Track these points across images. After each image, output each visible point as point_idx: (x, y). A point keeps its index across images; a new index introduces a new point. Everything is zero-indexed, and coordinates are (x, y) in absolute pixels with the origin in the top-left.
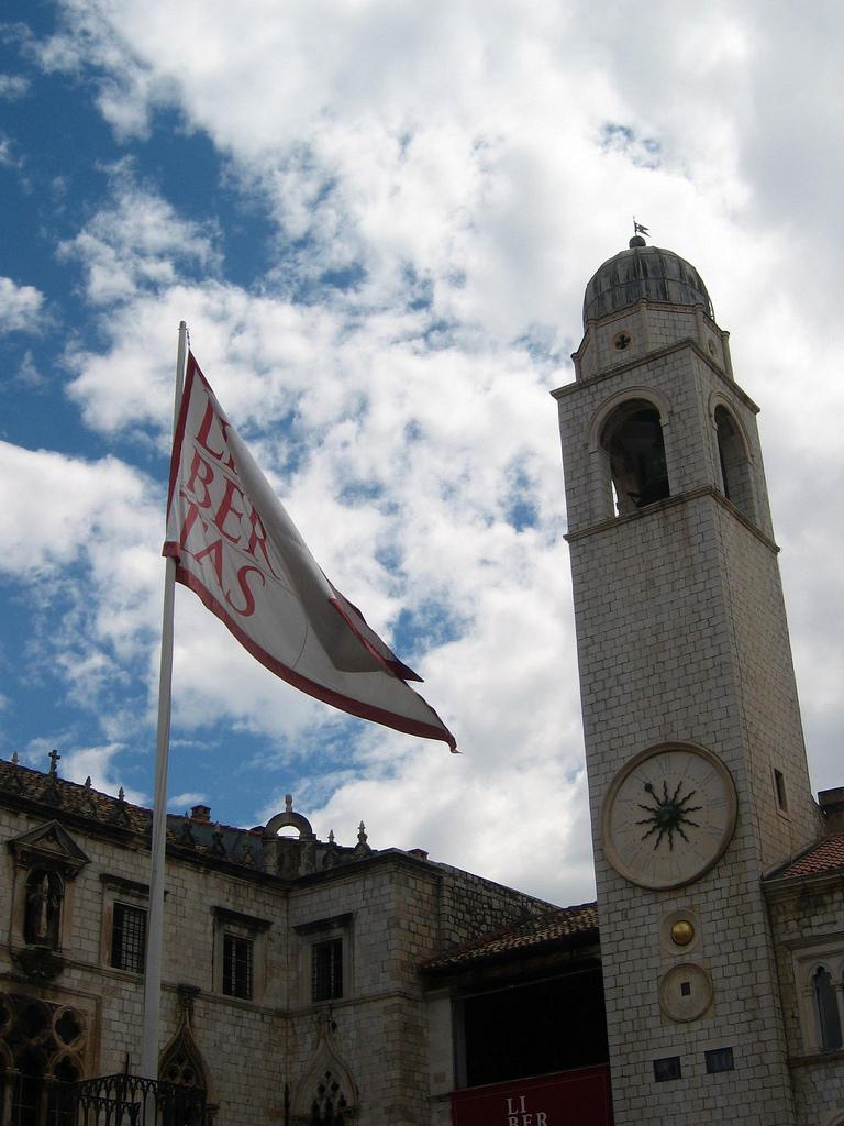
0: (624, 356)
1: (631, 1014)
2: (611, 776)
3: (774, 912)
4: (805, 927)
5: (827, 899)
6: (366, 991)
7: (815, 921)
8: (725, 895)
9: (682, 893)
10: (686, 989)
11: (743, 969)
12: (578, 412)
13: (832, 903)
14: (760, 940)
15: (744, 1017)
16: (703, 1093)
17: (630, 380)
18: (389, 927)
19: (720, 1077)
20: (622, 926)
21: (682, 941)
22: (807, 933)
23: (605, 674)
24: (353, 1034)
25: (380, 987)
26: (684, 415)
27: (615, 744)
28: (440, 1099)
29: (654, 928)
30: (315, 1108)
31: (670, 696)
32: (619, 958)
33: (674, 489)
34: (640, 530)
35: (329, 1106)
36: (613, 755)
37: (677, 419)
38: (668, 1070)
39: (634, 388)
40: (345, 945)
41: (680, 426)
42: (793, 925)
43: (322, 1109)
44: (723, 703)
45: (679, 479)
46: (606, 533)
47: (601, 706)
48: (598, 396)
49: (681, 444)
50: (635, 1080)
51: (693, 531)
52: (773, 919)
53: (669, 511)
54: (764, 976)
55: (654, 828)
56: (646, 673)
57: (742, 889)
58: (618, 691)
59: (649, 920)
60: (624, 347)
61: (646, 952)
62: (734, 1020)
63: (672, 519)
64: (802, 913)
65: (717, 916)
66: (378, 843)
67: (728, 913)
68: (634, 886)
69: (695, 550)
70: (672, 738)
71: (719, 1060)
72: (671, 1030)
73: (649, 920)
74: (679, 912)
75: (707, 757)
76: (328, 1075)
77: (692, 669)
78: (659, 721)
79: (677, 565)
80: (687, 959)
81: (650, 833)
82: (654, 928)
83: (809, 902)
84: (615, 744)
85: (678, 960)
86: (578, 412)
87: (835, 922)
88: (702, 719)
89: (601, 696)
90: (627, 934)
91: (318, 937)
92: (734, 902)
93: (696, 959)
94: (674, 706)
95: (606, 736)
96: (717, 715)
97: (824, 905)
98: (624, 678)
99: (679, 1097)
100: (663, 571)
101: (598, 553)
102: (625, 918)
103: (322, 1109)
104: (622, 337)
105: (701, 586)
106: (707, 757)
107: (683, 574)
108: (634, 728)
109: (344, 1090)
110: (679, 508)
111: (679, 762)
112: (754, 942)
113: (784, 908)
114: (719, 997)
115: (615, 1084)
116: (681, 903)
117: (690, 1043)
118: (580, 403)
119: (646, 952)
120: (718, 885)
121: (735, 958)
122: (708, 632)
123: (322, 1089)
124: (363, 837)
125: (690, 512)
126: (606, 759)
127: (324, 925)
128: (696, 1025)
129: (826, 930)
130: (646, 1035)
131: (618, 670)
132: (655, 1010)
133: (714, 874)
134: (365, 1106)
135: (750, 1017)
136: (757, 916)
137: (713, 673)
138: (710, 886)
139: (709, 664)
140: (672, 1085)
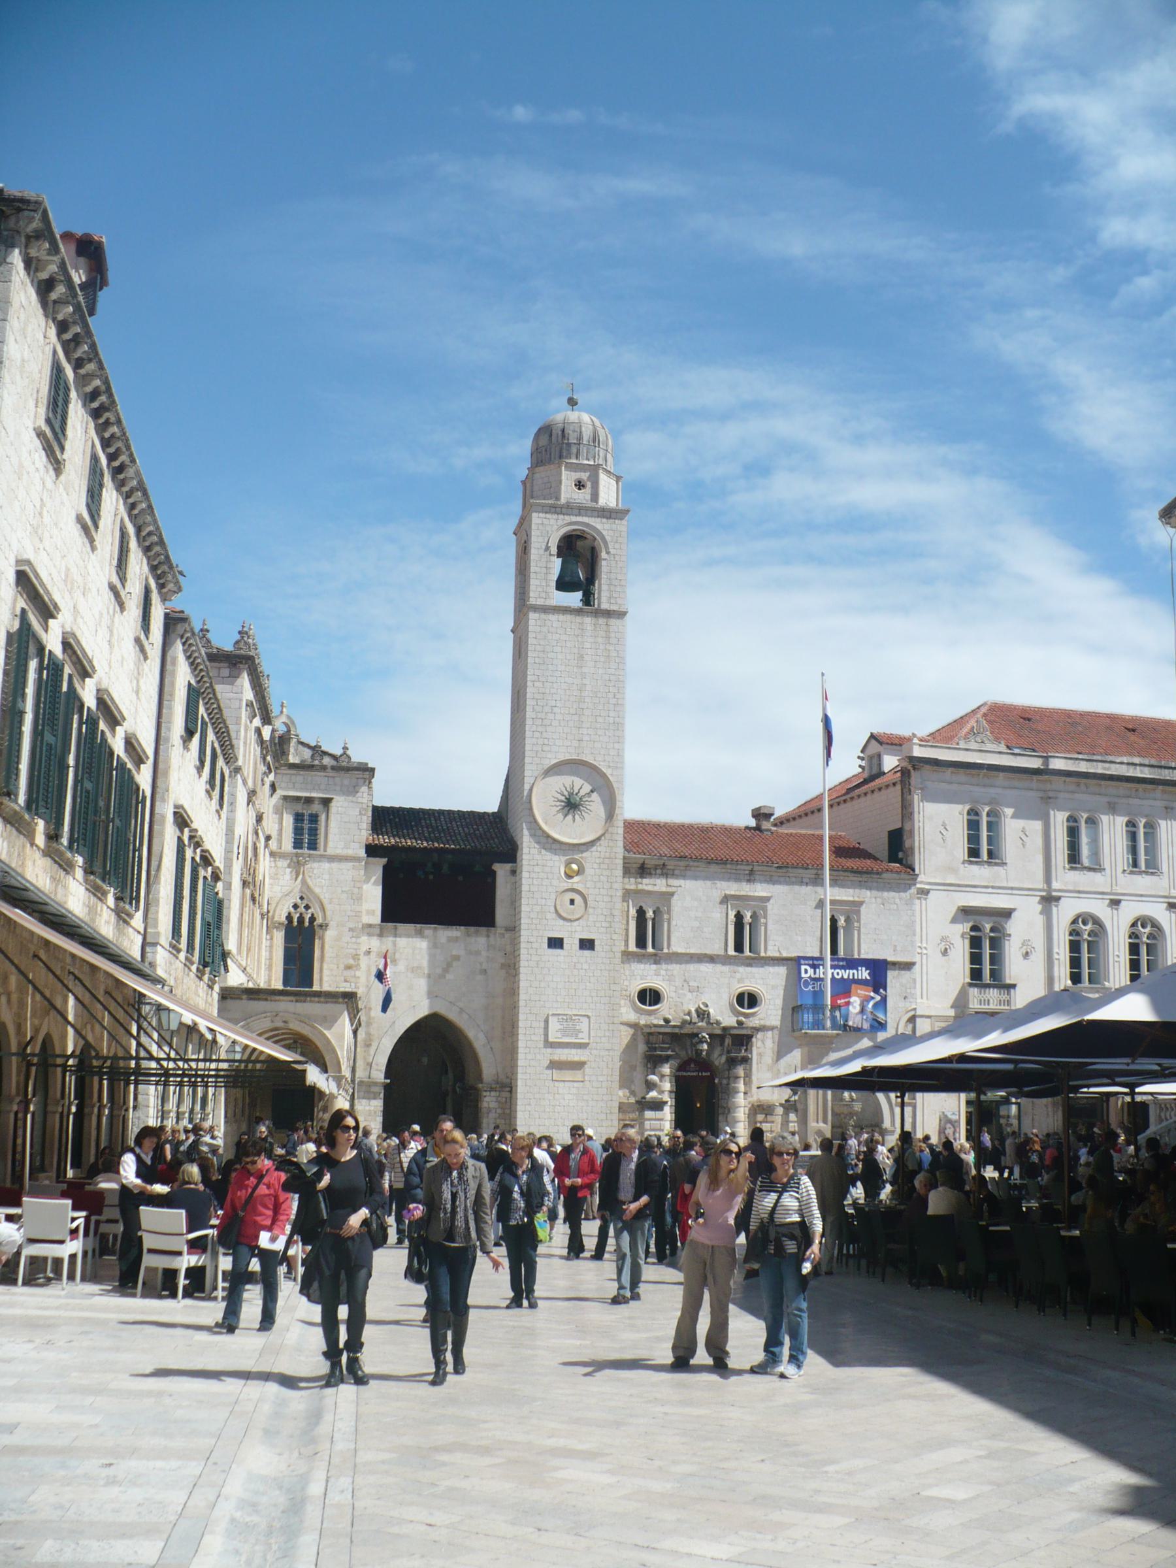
1: (538, 908)
6: (339, 852)
7: (645, 881)
8: (602, 855)
10: (572, 902)
11: (607, 899)
15: (604, 924)
16: (575, 960)
18: (361, 814)
19: (587, 953)
24: (326, 877)
25: (350, 852)
26: (617, 558)
27: (545, 748)
28: (370, 926)
30: (289, 917)
32: (533, 875)
35: (301, 919)
38: (556, 943)
39: (587, 525)
40: (323, 817)
41: (613, 563)
43: (295, 920)
44: (616, 745)
47: (539, 722)
48: (561, 517)
49: (613, 576)
50: (534, 945)
51: (613, 635)
57: (613, 855)
58: (551, 716)
62: (598, 924)
65: (596, 866)
66: (356, 757)
67: (603, 866)
69: (612, 648)
71: (587, 944)
72: (561, 922)
75: (604, 775)
76: (302, 898)
77: (600, 720)
80: (575, 886)
84: (545, 748)
88: (603, 752)
91: (299, 808)
92: (607, 861)
94: (586, 738)
95: (540, 741)
97: (650, 874)
99: (561, 959)
100: (589, 652)
103: (295, 920)
107: (602, 659)
109: (315, 910)
114: (591, 911)
115: (523, 945)
117: (571, 935)
119: (550, 876)
121: (603, 892)
122: (613, 701)
123: (295, 906)
124: (345, 748)
127: (309, 800)
128: (576, 923)
130: (545, 922)
131: (553, 703)
132: (553, 909)
134: (332, 924)
135: (607, 925)
138: (594, 848)
139: (611, 720)
140: (558, 951)
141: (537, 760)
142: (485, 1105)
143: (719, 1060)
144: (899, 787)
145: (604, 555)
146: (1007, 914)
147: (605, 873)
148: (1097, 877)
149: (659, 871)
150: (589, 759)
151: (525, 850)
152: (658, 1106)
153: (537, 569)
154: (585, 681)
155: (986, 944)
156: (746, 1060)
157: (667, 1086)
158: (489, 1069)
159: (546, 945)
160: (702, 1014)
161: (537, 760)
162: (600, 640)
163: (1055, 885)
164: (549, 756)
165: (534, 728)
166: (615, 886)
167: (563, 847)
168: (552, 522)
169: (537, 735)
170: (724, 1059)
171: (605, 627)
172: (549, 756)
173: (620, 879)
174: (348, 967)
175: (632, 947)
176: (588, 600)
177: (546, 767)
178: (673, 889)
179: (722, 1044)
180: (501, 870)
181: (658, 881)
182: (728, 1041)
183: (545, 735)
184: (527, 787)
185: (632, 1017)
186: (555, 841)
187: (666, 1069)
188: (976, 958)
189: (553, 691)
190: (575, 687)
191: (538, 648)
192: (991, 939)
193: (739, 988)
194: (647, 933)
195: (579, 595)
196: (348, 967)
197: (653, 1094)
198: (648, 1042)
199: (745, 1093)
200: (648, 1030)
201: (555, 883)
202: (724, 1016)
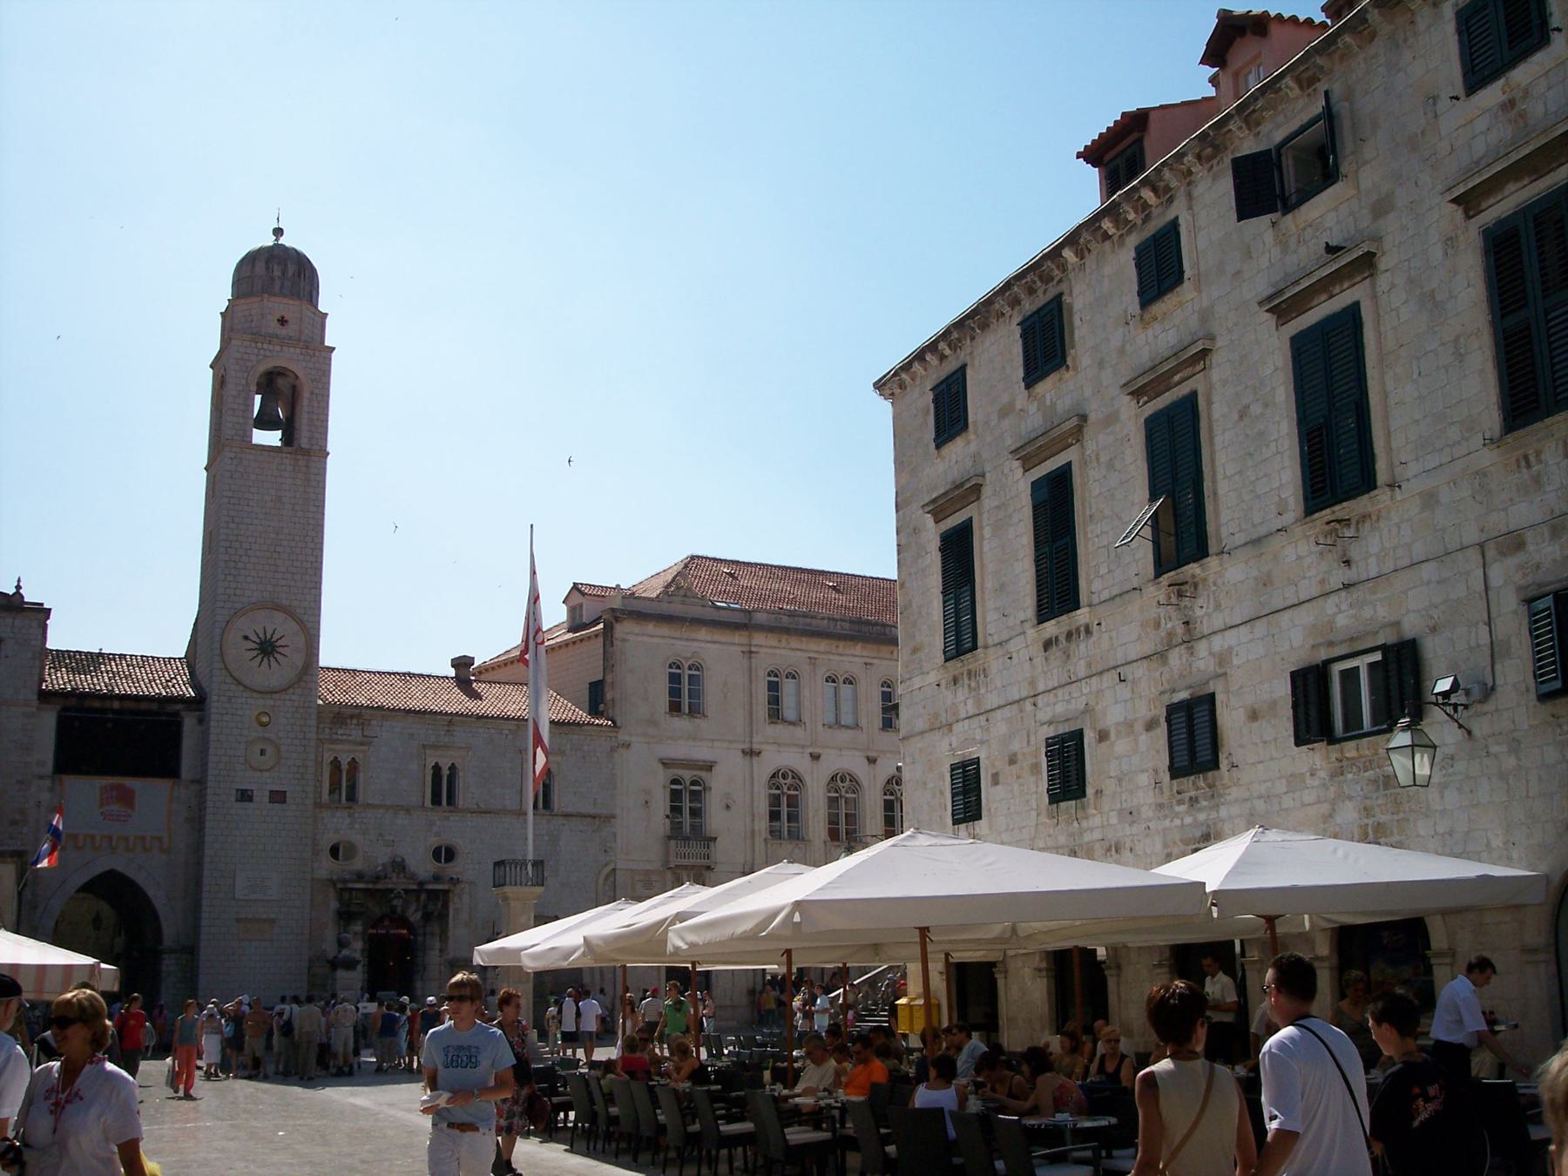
0: (283, 331)
10: (263, 752)
14: (312, 736)
21: (264, 725)
23: (237, 545)
28: (41, 777)
38: (245, 796)
45: (310, 439)
54: (312, 757)
66: (30, 596)
69: (310, 490)
71: (278, 797)
75: (300, 622)
78: (269, 588)
95: (233, 585)
102: (230, 698)
106: (300, 622)
111: (279, 617)
117: (262, 785)
121: (296, 742)
124: (18, 587)
136: (314, 722)
142: (164, 968)
143: (415, 916)
144: (601, 639)
146: (709, 767)
148: (799, 732)
150: (285, 602)
151: (215, 698)
152: (350, 964)
155: (686, 797)
156: (443, 917)
157: (358, 945)
158: (171, 929)
159: (233, 799)
160: (399, 866)
162: (299, 482)
163: (756, 739)
168: (253, 358)
170: (419, 915)
173: (314, 729)
174: (14, 823)
175: (325, 796)
176: (288, 439)
179: (418, 899)
180: (189, 722)
182: (423, 897)
185: (322, 873)
187: (358, 927)
188: (676, 810)
192: (693, 793)
193: (434, 841)
194: (344, 784)
195: (279, 433)
196: (14, 823)
197: (345, 952)
198: (340, 899)
199: (441, 950)
200: (340, 886)
202: (422, 866)
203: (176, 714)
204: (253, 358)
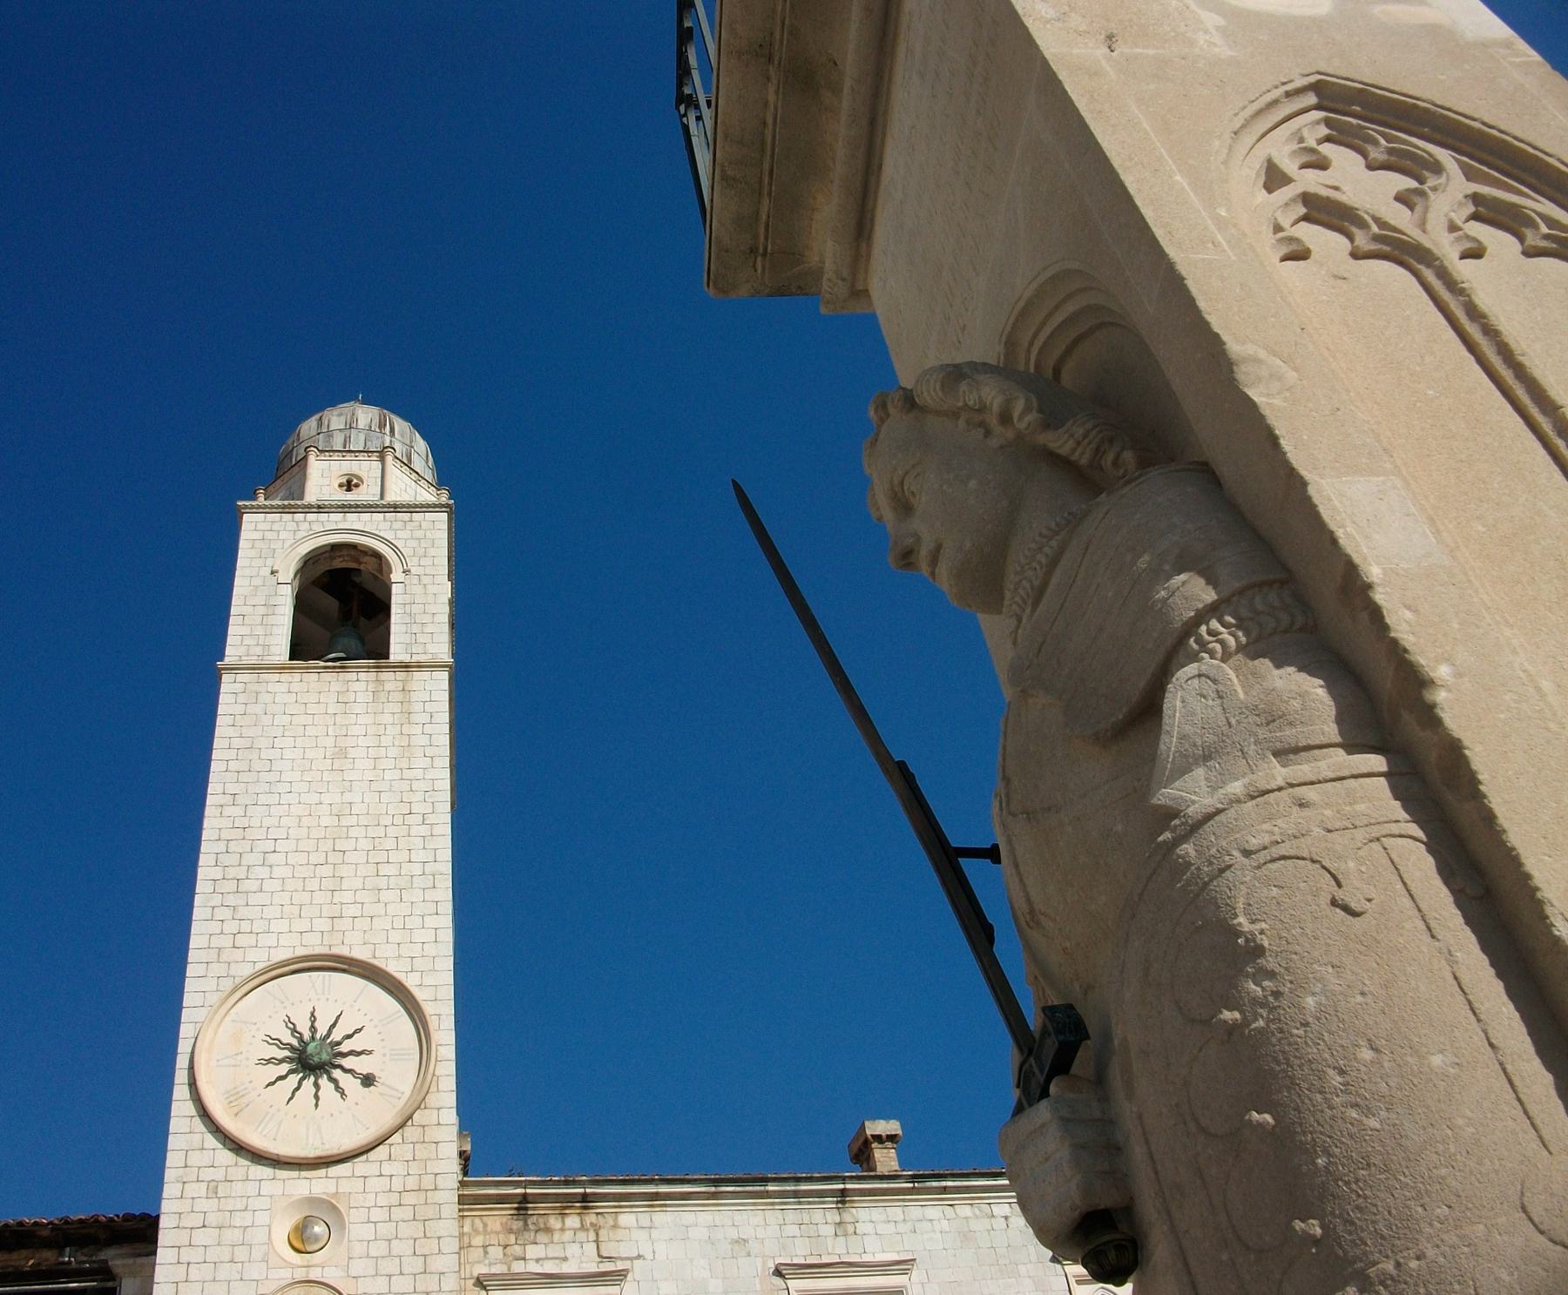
0: (351, 497)
2: (227, 985)
3: (466, 1229)
4: (517, 1259)
5: (554, 1222)
7: (532, 1251)
8: (397, 1184)
9: (322, 1172)
12: (269, 535)
13: (563, 1230)
14: (447, 1262)
17: (354, 520)
20: (202, 1205)
22: (518, 1267)
26: (425, 580)
27: (240, 940)
29: (262, 1218)
31: (347, 897)
33: (397, 653)
34: (335, 687)
36: (238, 954)
37: (415, 581)
39: (363, 533)
41: (418, 589)
42: (496, 1252)
46: (285, 677)
48: (305, 526)
49: (416, 609)
51: (418, 707)
52: (466, 1240)
53: (386, 676)
55: (291, 1072)
56: (314, 859)
57: (428, 1182)
58: (263, 872)
59: (255, 1203)
60: (349, 490)
61: (241, 1253)
63: (388, 686)
64: (512, 1237)
67: (398, 1213)
68: (238, 1147)
69: (418, 730)
70: (344, 951)
73: (255, 1203)
74: (312, 1201)
77: (384, 870)
79: (386, 741)
80: (315, 1274)
81: (349, 1037)
82: (262, 1218)
83: (526, 1224)
84: (240, 940)
85: (300, 1274)
86: (269, 535)
87: (565, 1259)
88: (395, 936)
89: (231, 873)
90: (212, 1219)
92: (409, 1199)
93: (332, 1275)
95: (231, 927)
96: (419, 936)
97: (548, 1230)
98: (272, 858)
100: (362, 741)
101: (265, 698)
104: (349, 482)
105: (418, 773)
107: (393, 752)
108: (282, 926)
110: (401, 675)
112: (437, 1264)
113: (485, 1225)
116: (318, 1184)
118: (275, 527)
119: (241, 1253)
120: (387, 1169)
122: (424, 830)
125: (413, 686)
126: (224, 958)
129: (550, 1268)
133: (382, 1151)
137: (418, 882)
138: (372, 1169)
141: (218, 969)
145: (396, 576)
147: (406, 1230)
149: (573, 1221)
153: (247, 610)
154: (348, 797)
161: (218, 969)
164: (252, 955)
165: (217, 900)
166: (437, 1264)
167: (283, 1174)
169: (221, 913)
171: (398, 696)
172: (252, 955)
173: (451, 1245)
177: (238, 981)
178: (620, 1266)
181: (572, 1250)
183: (243, 912)
184: (186, 1031)
186: (258, 1157)
189: (267, 822)
190: (325, 809)
191: (236, 743)
201: (255, 1272)
203: (105, 1273)
204: (283, 535)
